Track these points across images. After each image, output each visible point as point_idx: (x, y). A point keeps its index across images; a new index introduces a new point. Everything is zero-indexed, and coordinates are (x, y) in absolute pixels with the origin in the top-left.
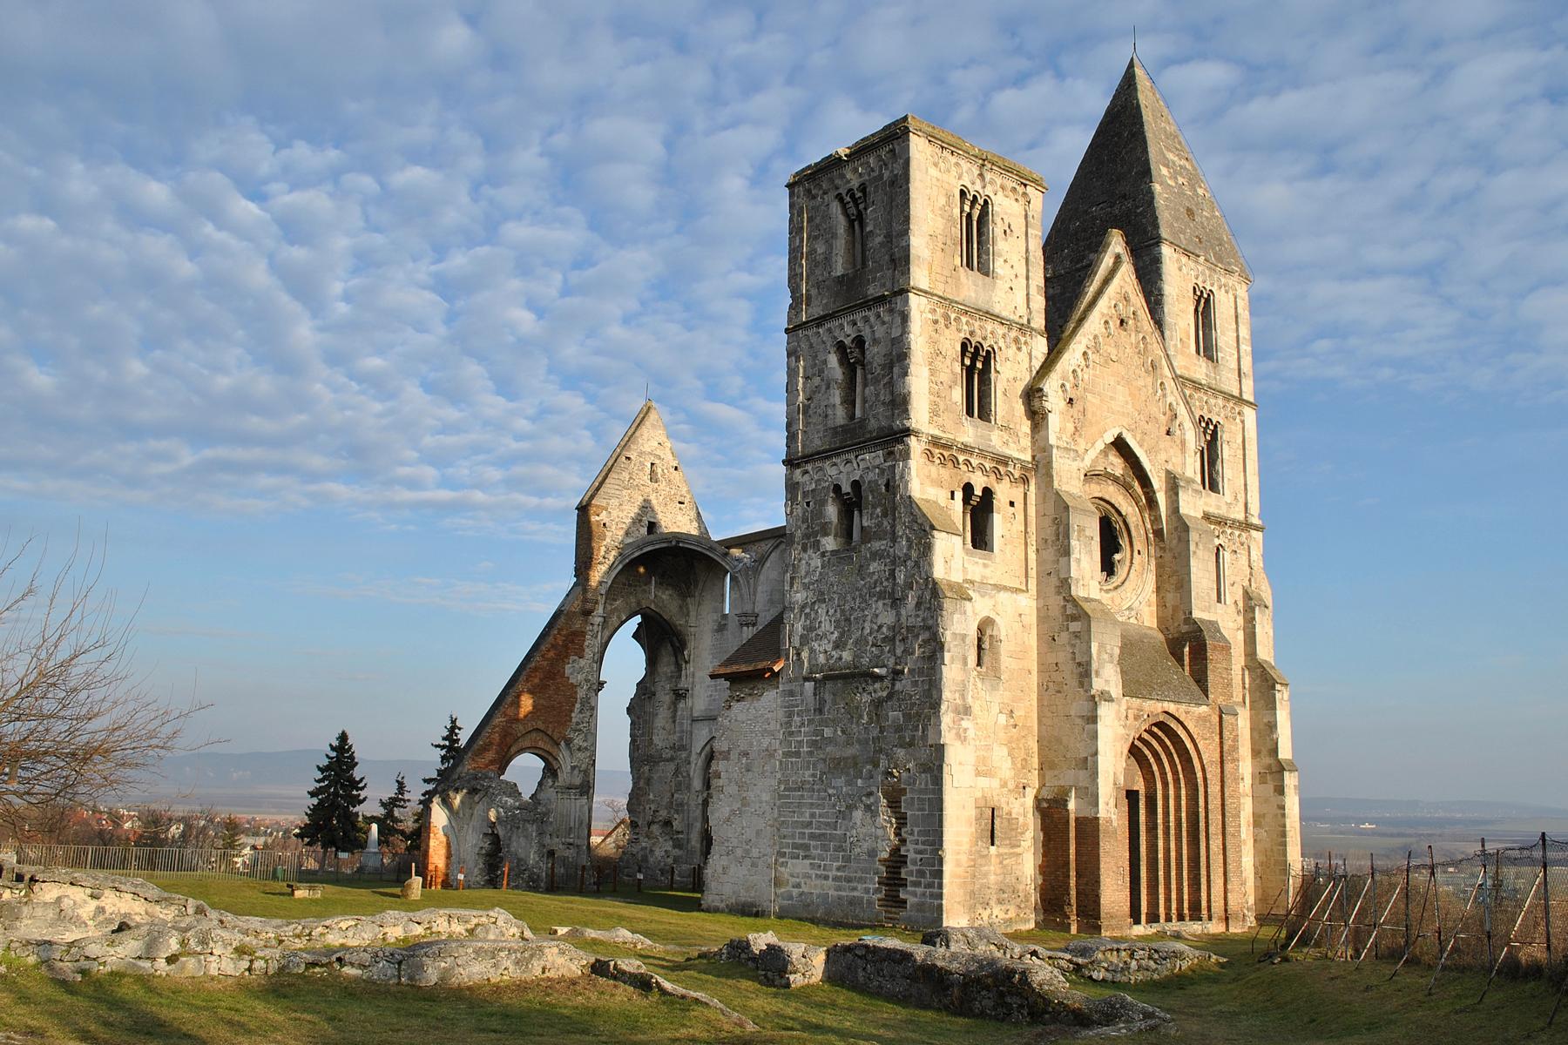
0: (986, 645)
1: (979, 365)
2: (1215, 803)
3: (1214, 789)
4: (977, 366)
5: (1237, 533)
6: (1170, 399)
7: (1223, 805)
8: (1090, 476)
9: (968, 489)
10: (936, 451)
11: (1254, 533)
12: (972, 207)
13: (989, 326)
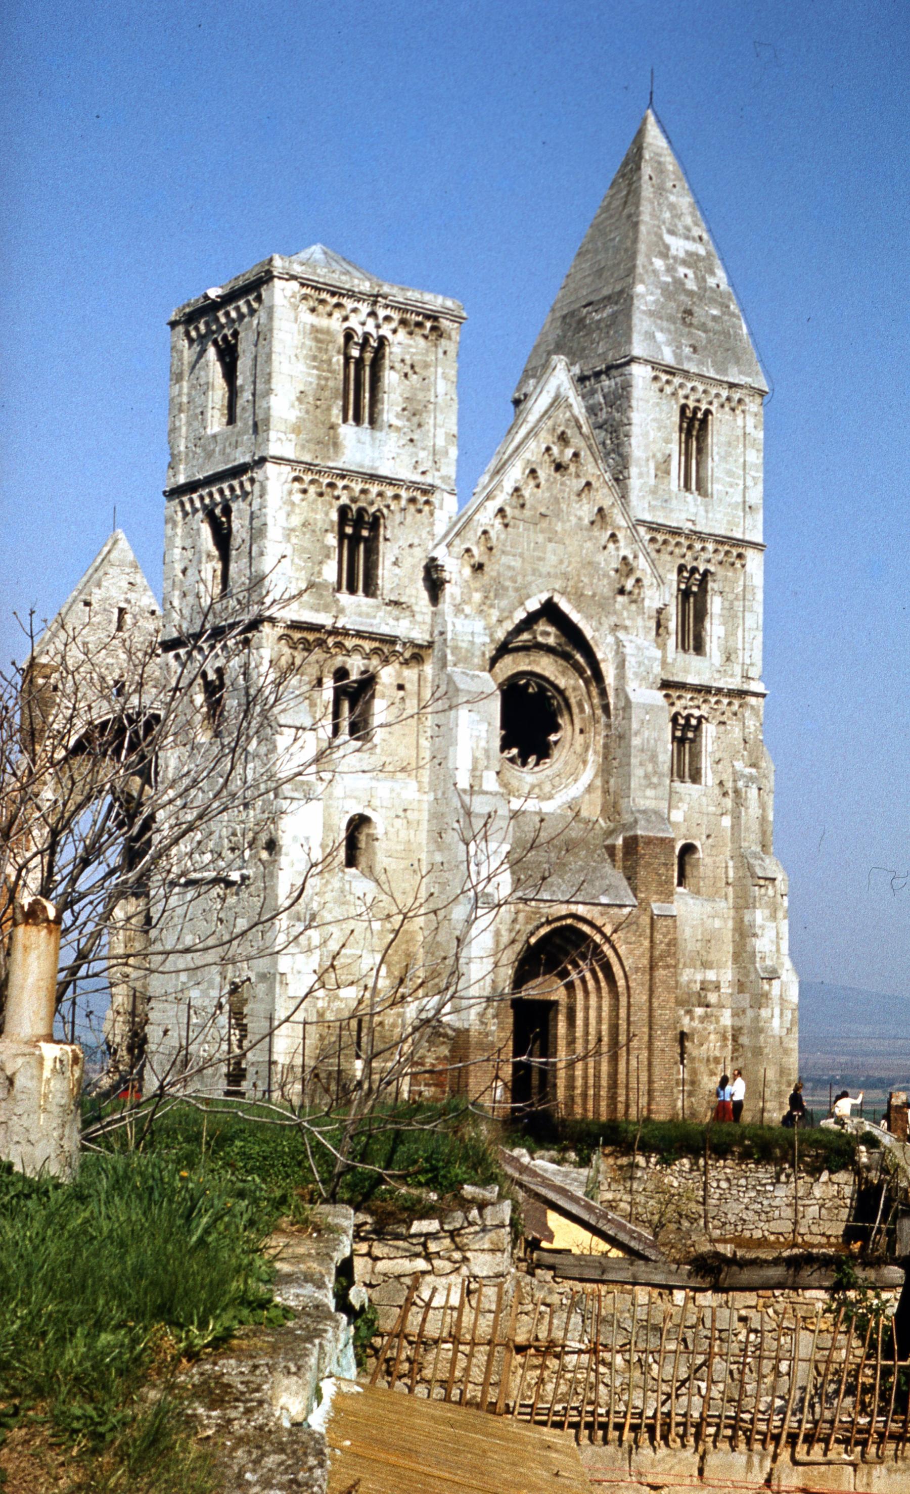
0: (362, 845)
1: (365, 533)
2: (640, 1016)
3: (640, 997)
4: (359, 535)
5: (725, 701)
6: (622, 553)
7: (651, 1016)
8: (503, 649)
9: (341, 673)
10: (297, 635)
11: (752, 700)
12: (362, 350)
13: (374, 489)
